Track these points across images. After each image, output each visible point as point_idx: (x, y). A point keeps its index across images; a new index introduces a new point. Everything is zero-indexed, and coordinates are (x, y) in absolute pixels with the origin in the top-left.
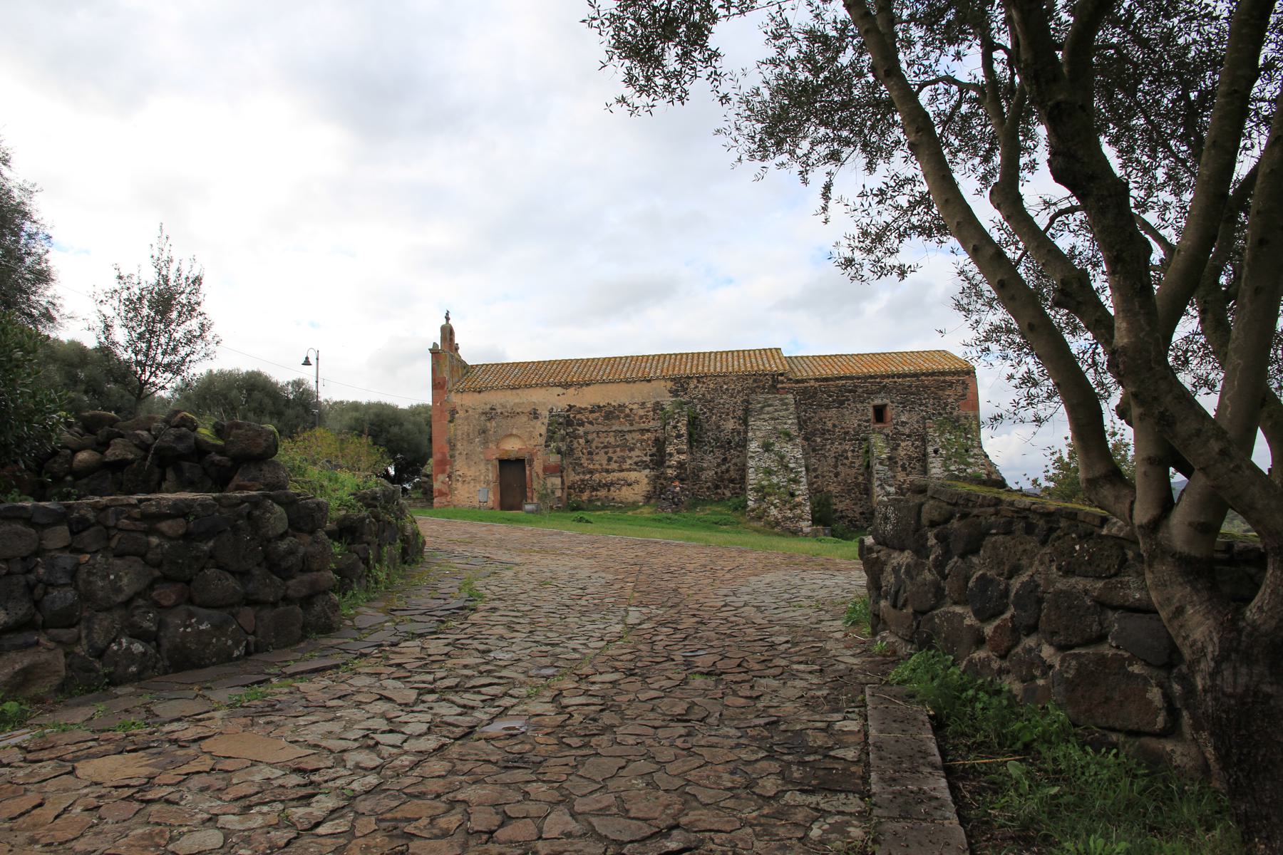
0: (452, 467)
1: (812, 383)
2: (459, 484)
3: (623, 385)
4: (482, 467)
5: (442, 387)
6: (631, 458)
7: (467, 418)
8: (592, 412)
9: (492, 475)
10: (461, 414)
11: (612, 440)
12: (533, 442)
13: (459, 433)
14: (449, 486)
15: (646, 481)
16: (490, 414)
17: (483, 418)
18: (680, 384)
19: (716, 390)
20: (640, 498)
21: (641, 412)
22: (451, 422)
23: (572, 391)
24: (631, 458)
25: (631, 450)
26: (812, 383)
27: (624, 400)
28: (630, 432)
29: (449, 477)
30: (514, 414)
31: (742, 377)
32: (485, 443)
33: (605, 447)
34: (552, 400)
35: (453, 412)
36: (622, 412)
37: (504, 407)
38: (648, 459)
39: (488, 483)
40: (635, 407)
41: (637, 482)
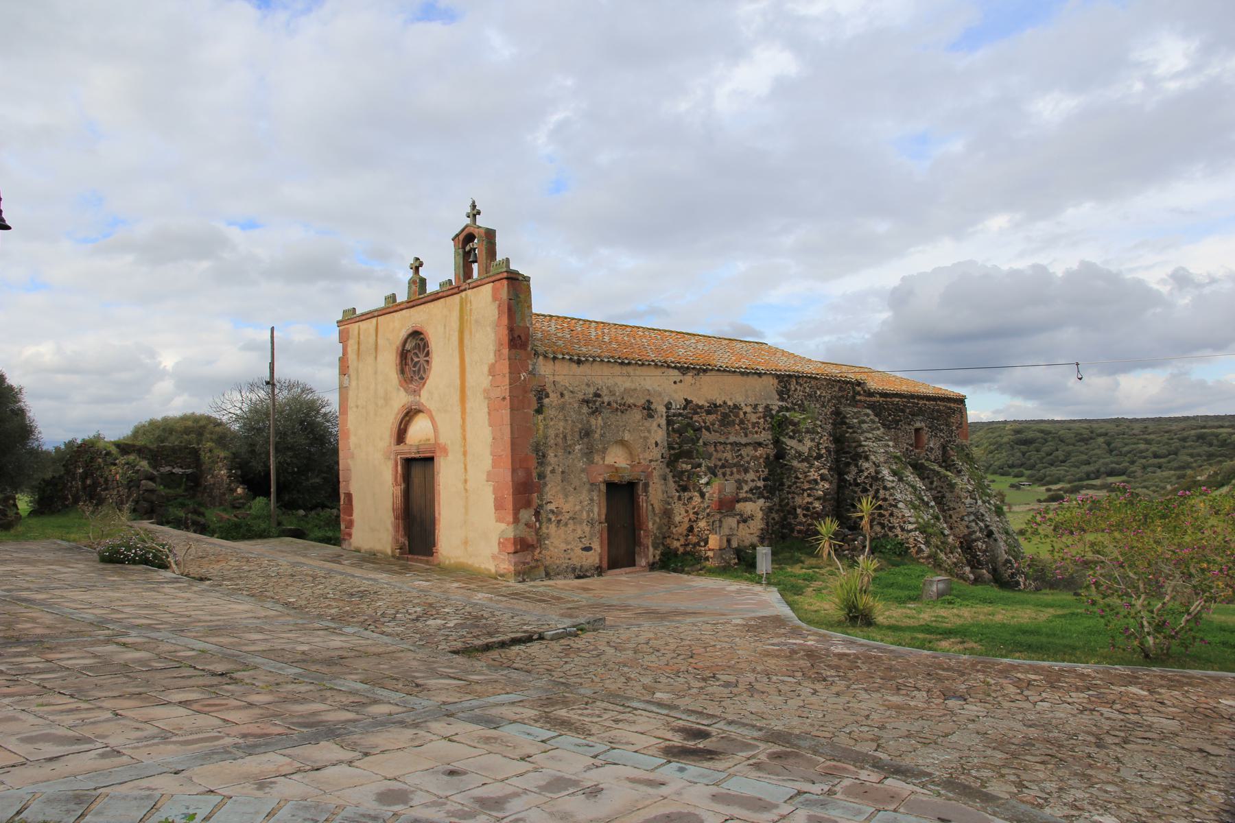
0: (541, 498)
1: (877, 398)
2: (553, 527)
3: (739, 378)
4: (584, 496)
5: (523, 346)
6: (746, 482)
7: (562, 408)
8: (709, 412)
9: (598, 510)
10: (552, 400)
11: (728, 455)
12: (648, 456)
13: (552, 433)
14: (537, 531)
15: (760, 515)
16: (594, 403)
17: (585, 410)
18: (786, 381)
19: (810, 396)
20: (755, 540)
21: (754, 418)
22: (539, 411)
23: (689, 378)
24: (746, 482)
25: (746, 471)
26: (877, 398)
27: (739, 399)
28: (746, 445)
29: (537, 514)
30: (625, 408)
31: (832, 382)
32: (589, 453)
33: (723, 466)
34: (670, 390)
35: (541, 394)
36: (737, 415)
37: (612, 393)
38: (761, 484)
39: (591, 523)
40: (749, 409)
41: (752, 517)
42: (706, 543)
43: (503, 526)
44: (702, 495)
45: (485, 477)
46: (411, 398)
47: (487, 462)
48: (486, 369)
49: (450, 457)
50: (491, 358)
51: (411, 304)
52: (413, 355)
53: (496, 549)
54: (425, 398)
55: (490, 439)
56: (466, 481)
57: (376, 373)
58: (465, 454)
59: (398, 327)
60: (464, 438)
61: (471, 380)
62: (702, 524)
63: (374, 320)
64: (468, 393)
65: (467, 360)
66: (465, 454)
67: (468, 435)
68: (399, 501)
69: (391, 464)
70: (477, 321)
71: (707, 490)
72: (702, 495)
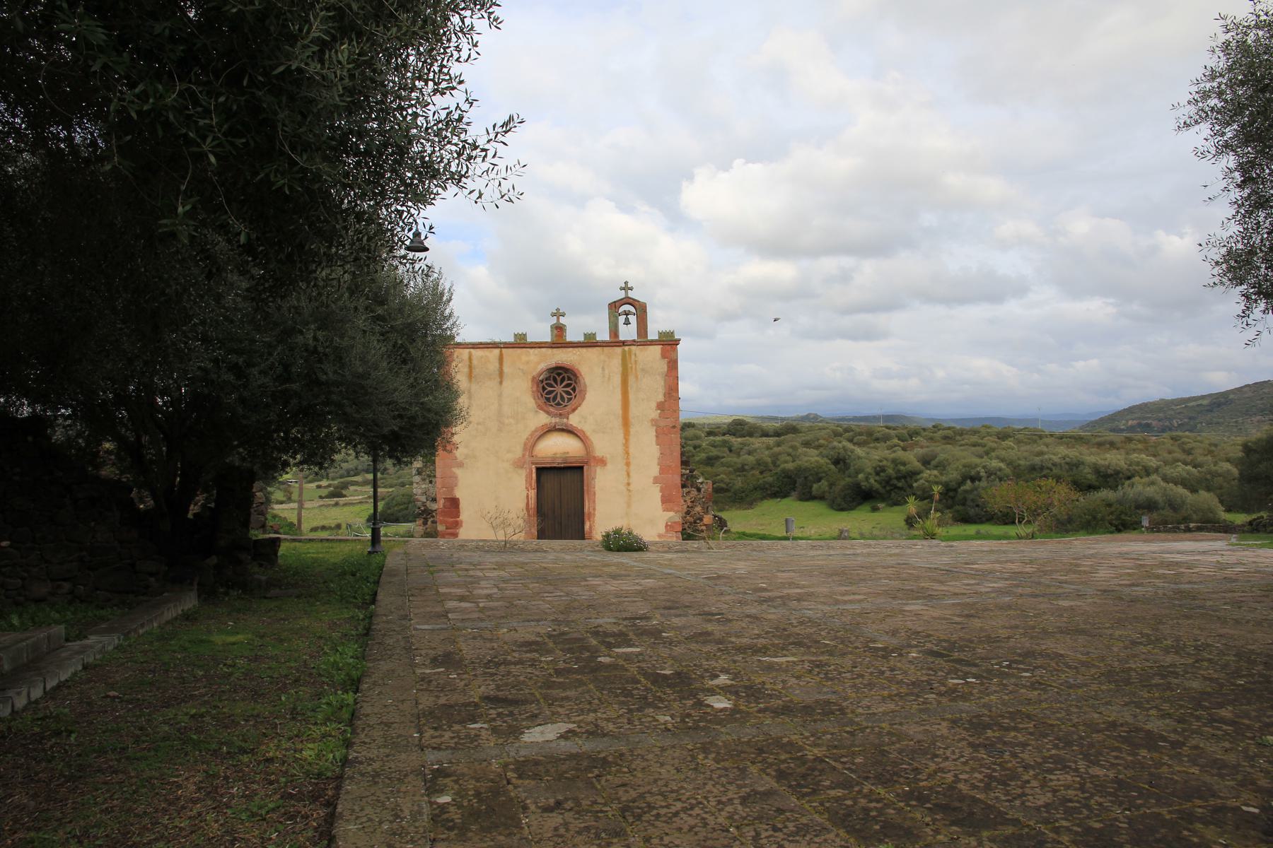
42: (701, 520)
43: (672, 514)
44: (699, 490)
45: (651, 480)
46: (554, 420)
47: (655, 470)
48: (654, 405)
49: (609, 466)
50: (661, 398)
51: (553, 345)
52: (559, 386)
53: (662, 530)
54: (574, 420)
55: (657, 454)
56: (629, 484)
57: (500, 395)
58: (628, 464)
59: (542, 361)
60: (627, 453)
61: (634, 410)
62: (698, 509)
63: (497, 351)
64: (632, 420)
65: (631, 397)
66: (628, 464)
67: (631, 450)
68: (533, 502)
69: (523, 473)
70: (643, 370)
71: (704, 488)
72: (699, 490)
